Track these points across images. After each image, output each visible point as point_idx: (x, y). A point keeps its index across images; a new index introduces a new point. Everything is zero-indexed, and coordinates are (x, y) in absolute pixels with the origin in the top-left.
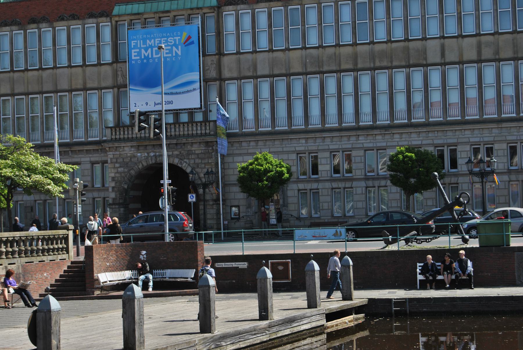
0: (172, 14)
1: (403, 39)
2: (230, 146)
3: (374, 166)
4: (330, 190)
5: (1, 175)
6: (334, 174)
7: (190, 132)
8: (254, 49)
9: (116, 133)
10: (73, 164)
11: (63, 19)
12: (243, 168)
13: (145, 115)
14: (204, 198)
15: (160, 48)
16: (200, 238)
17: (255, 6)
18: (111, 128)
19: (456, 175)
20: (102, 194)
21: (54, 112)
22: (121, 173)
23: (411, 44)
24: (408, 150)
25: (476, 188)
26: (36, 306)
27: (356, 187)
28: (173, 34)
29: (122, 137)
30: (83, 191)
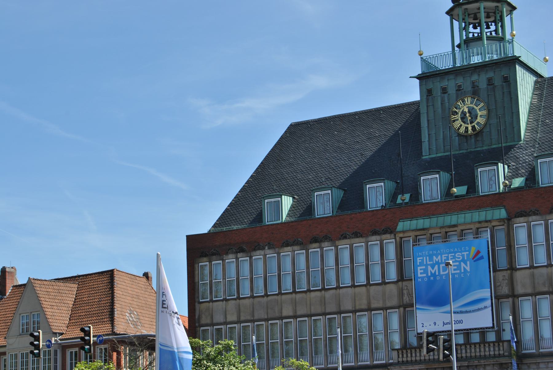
0: (459, 229)
7: (482, 354)
8: (549, 263)
9: (403, 355)
11: (345, 238)
13: (433, 336)
15: (448, 264)
17: (548, 217)
18: (397, 350)
21: (337, 334)
28: (461, 249)
29: (409, 359)
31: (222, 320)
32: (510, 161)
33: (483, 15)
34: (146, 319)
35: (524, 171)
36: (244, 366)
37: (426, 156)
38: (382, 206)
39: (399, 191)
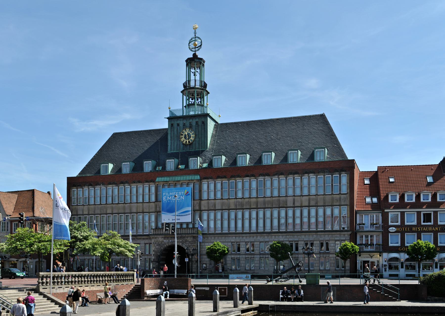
0: (181, 182)
1: (278, 196)
2: (203, 238)
3: (264, 249)
4: (245, 258)
5: (107, 248)
6: (247, 252)
7: (187, 232)
9: (155, 231)
10: (137, 244)
11: (135, 183)
12: (208, 248)
13: (168, 224)
14: (192, 260)
15: (175, 196)
17: (216, 180)
18: (153, 229)
20: (149, 257)
22: (157, 248)
23: (281, 198)
24: (278, 243)
25: (306, 260)
26: (120, 303)
27: (256, 258)
29: (158, 233)
32: (203, 157)
33: (196, 94)
34: (49, 211)
35: (208, 161)
36: (90, 233)
37: (169, 151)
38: (150, 171)
39: (157, 165)
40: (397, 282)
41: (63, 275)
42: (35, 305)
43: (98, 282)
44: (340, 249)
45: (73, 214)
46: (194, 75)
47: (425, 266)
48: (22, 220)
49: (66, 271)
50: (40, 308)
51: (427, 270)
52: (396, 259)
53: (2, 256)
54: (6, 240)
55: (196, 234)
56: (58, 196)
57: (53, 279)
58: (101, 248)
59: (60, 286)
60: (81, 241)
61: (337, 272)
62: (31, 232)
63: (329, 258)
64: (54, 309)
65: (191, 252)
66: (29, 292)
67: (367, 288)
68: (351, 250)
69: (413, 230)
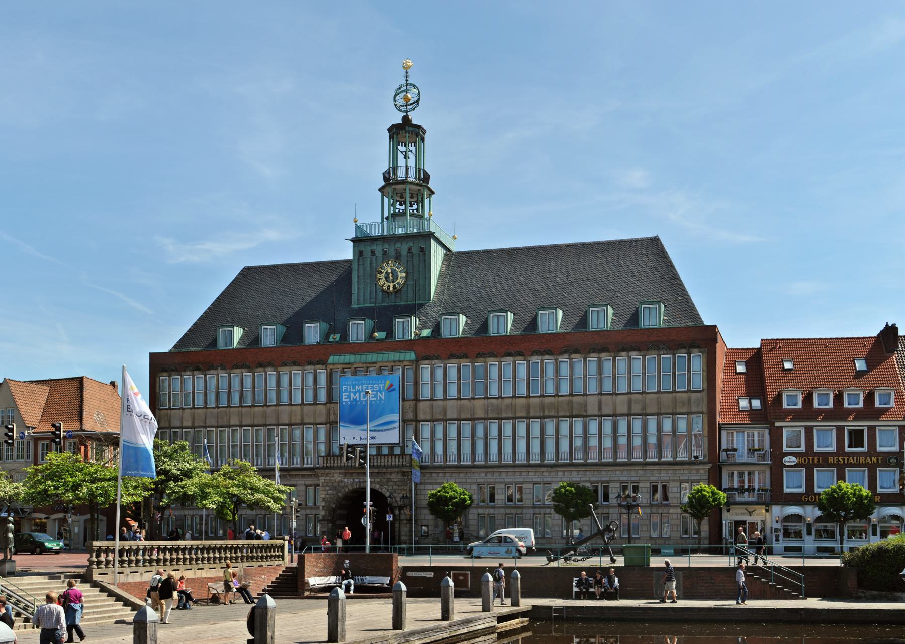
0: (377, 365)
2: (423, 475)
3: (542, 498)
7: (390, 463)
8: (445, 397)
11: (286, 365)
12: (432, 494)
13: (352, 448)
15: (367, 393)
16: (395, 551)
17: (447, 362)
18: (323, 457)
19: (608, 507)
20: (314, 512)
22: (330, 495)
24: (570, 485)
26: (255, 603)
28: (378, 382)
29: (332, 465)
30: (298, 508)
31: (179, 425)
36: (196, 463)
38: (317, 342)
40: (800, 563)
41: (141, 548)
42: (82, 608)
43: (211, 561)
44: (689, 498)
45: (162, 425)
46: (405, 158)
47: (853, 531)
48: (59, 436)
49: (146, 539)
50: (94, 612)
51: (857, 538)
52: (798, 518)
53: (17, 509)
54: (25, 476)
55: (408, 466)
56: (132, 389)
57: (121, 555)
58: (217, 493)
59: (134, 569)
60: (177, 479)
61: (684, 541)
62: (77, 461)
63: (668, 515)
64: (122, 615)
65: (397, 503)
66: (71, 580)
67: (742, 573)
68: (711, 500)
69: (829, 462)
